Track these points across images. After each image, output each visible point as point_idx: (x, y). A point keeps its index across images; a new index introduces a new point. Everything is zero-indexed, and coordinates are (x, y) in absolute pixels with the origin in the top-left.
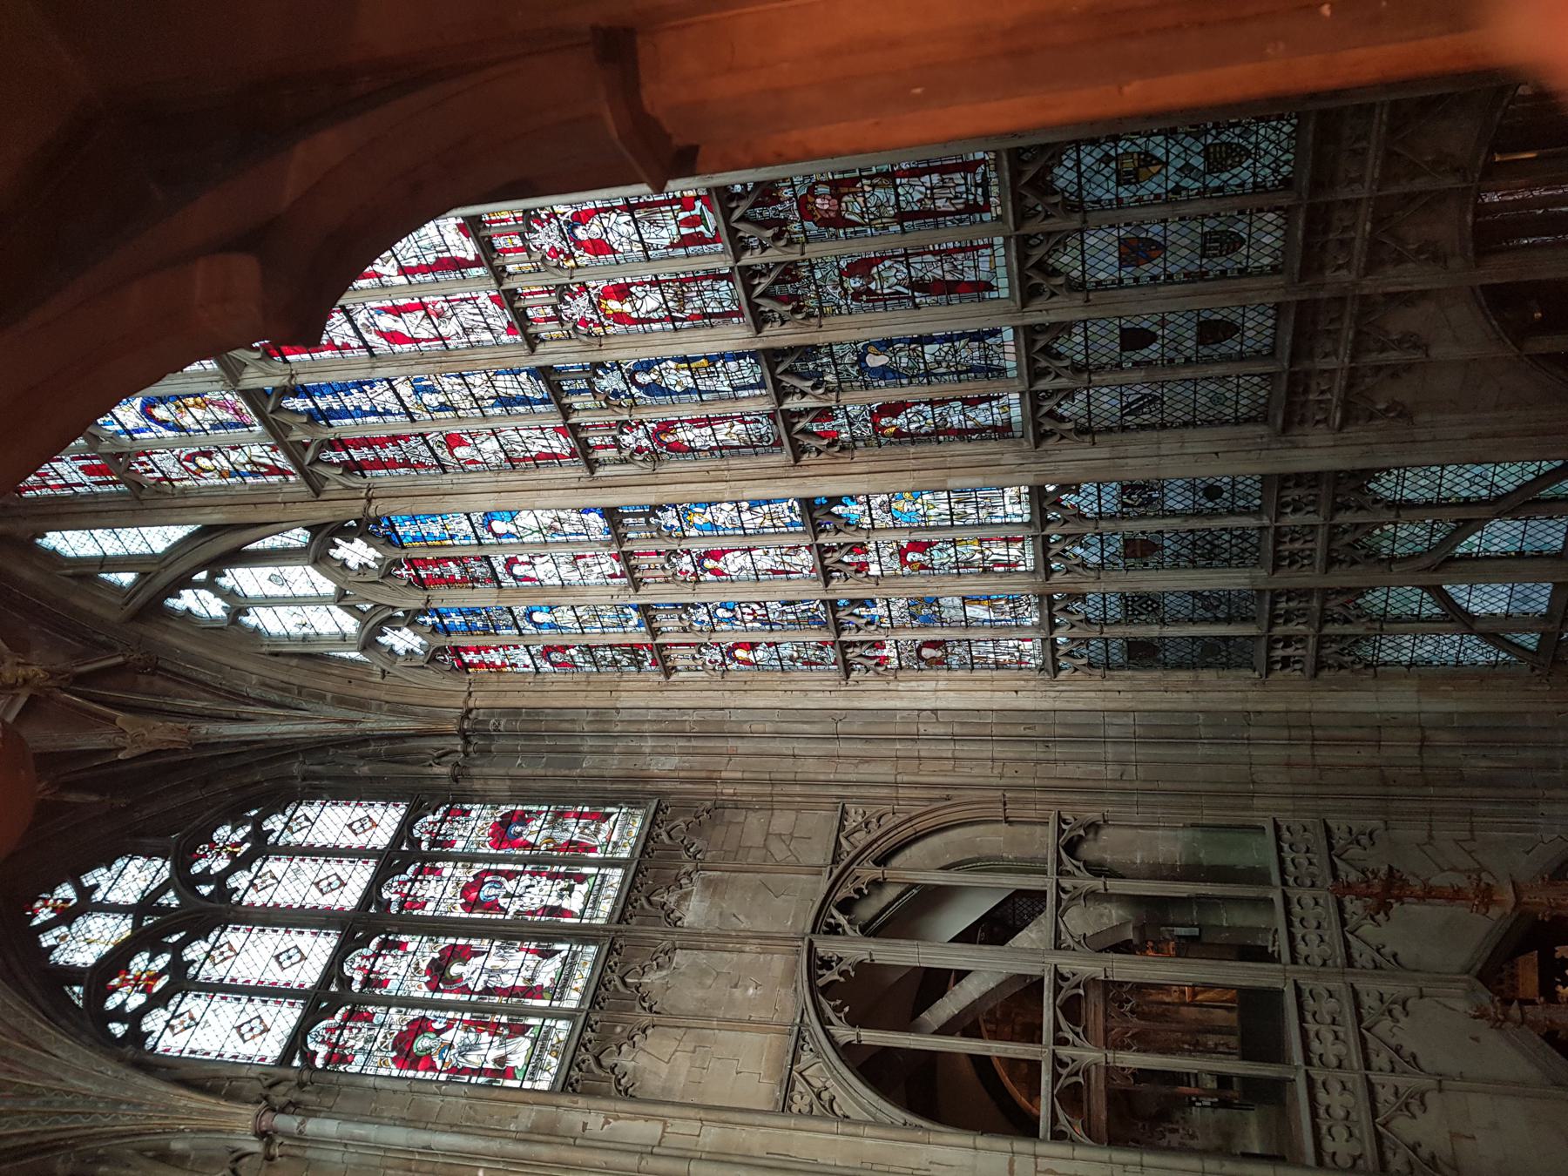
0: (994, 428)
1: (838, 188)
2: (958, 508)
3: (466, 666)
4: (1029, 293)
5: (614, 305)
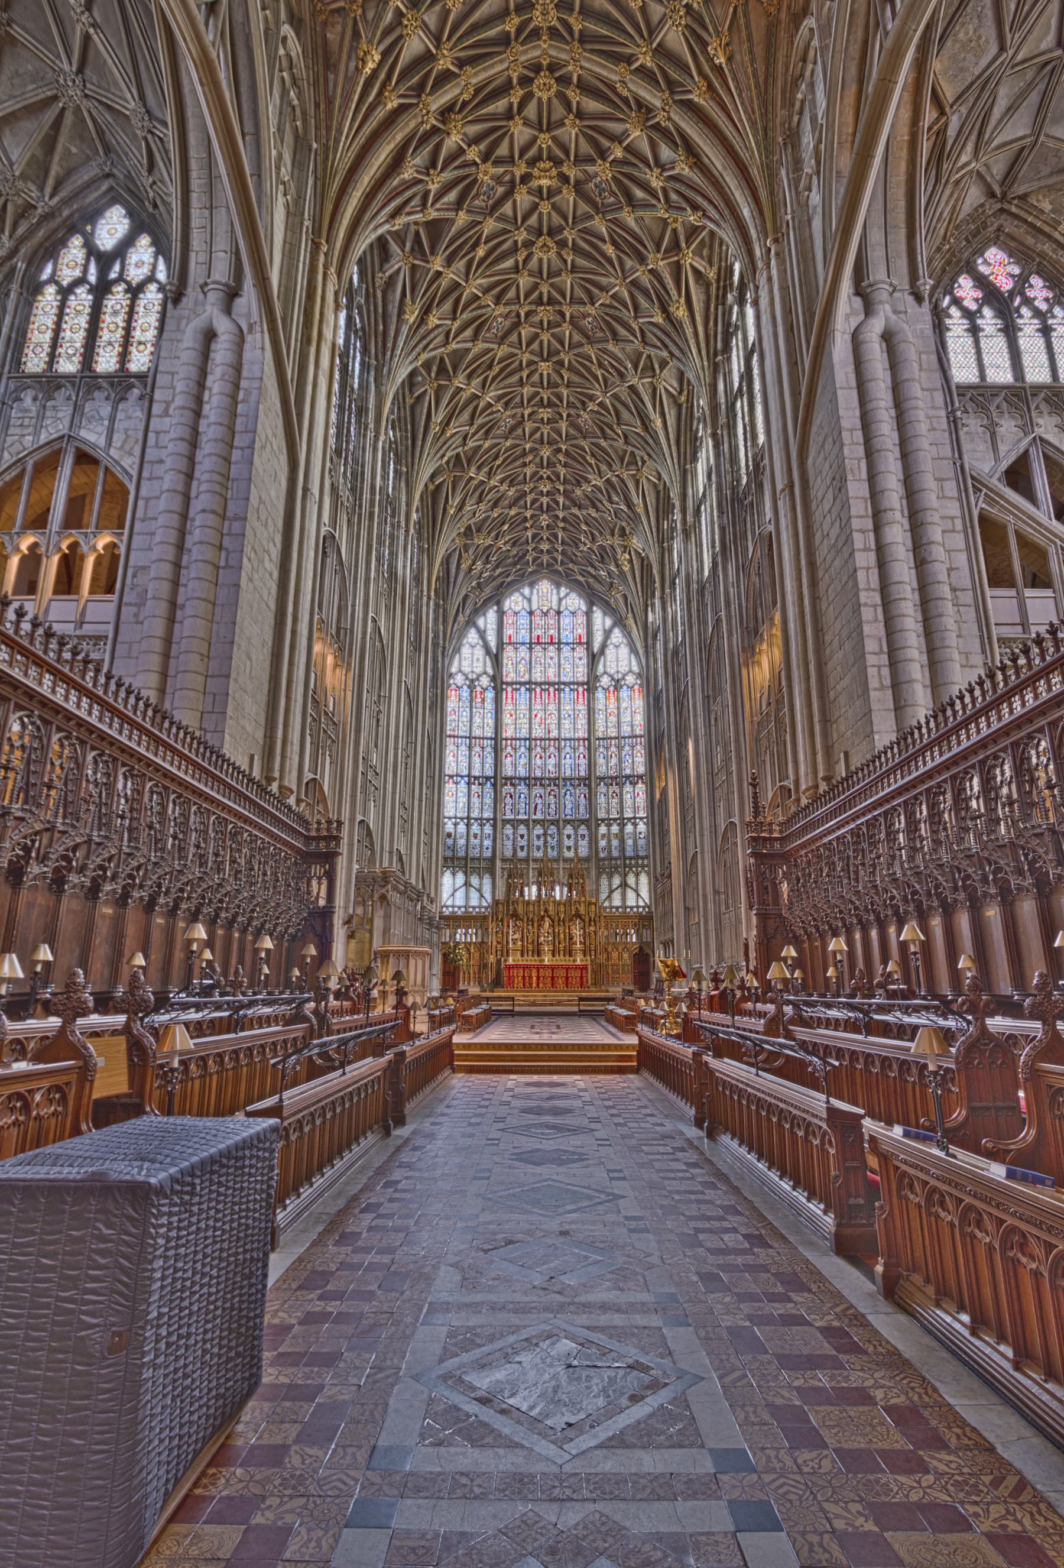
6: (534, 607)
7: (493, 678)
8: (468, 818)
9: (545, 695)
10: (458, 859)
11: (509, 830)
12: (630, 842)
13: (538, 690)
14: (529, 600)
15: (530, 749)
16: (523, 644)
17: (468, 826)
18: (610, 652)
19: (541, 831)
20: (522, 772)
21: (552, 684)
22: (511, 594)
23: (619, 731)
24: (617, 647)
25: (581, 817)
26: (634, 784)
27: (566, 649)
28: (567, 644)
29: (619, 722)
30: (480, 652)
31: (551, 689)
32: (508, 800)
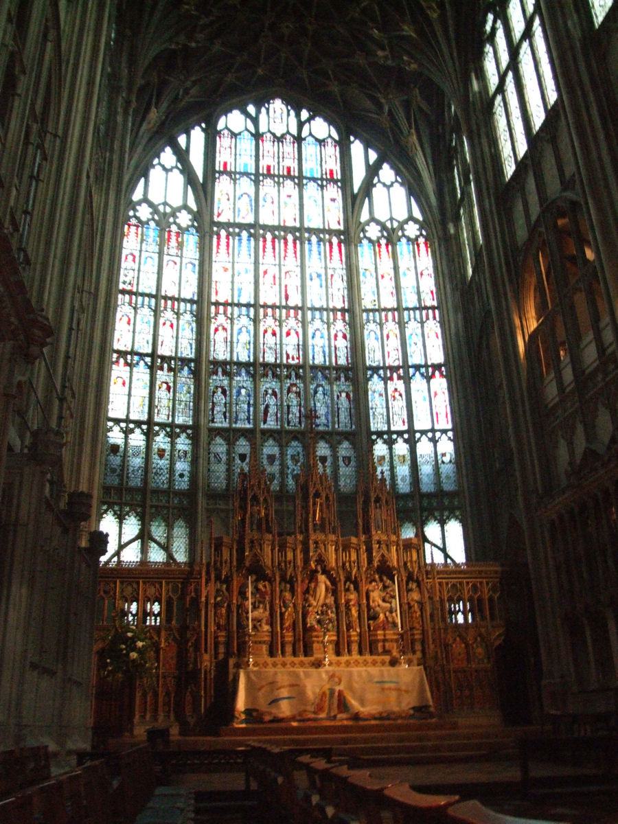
0: (213, 419)
1: (298, 394)
2: (183, 404)
3: (129, 225)
4: (264, 432)
5: (270, 331)
6: (263, 128)
7: (197, 216)
8: (150, 422)
9: (280, 245)
10: (131, 490)
11: (220, 446)
12: (426, 469)
13: (269, 236)
14: (255, 121)
15: (256, 321)
16: (247, 174)
17: (149, 436)
18: (378, 192)
19: (275, 451)
20: (243, 355)
21: (293, 230)
22: (227, 111)
23: (399, 300)
24: (388, 187)
25: (342, 428)
26: (428, 378)
27: (311, 189)
28: (314, 180)
29: (398, 287)
30: (177, 179)
31: (290, 238)
32: (219, 397)
